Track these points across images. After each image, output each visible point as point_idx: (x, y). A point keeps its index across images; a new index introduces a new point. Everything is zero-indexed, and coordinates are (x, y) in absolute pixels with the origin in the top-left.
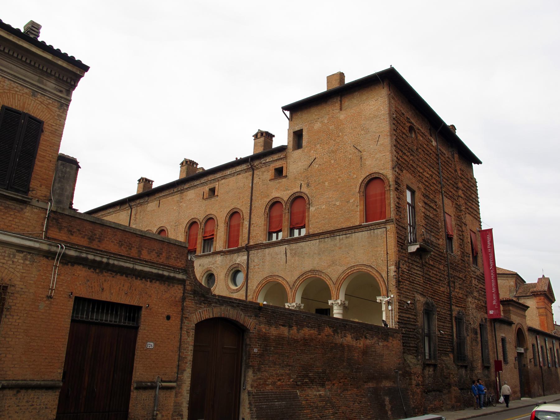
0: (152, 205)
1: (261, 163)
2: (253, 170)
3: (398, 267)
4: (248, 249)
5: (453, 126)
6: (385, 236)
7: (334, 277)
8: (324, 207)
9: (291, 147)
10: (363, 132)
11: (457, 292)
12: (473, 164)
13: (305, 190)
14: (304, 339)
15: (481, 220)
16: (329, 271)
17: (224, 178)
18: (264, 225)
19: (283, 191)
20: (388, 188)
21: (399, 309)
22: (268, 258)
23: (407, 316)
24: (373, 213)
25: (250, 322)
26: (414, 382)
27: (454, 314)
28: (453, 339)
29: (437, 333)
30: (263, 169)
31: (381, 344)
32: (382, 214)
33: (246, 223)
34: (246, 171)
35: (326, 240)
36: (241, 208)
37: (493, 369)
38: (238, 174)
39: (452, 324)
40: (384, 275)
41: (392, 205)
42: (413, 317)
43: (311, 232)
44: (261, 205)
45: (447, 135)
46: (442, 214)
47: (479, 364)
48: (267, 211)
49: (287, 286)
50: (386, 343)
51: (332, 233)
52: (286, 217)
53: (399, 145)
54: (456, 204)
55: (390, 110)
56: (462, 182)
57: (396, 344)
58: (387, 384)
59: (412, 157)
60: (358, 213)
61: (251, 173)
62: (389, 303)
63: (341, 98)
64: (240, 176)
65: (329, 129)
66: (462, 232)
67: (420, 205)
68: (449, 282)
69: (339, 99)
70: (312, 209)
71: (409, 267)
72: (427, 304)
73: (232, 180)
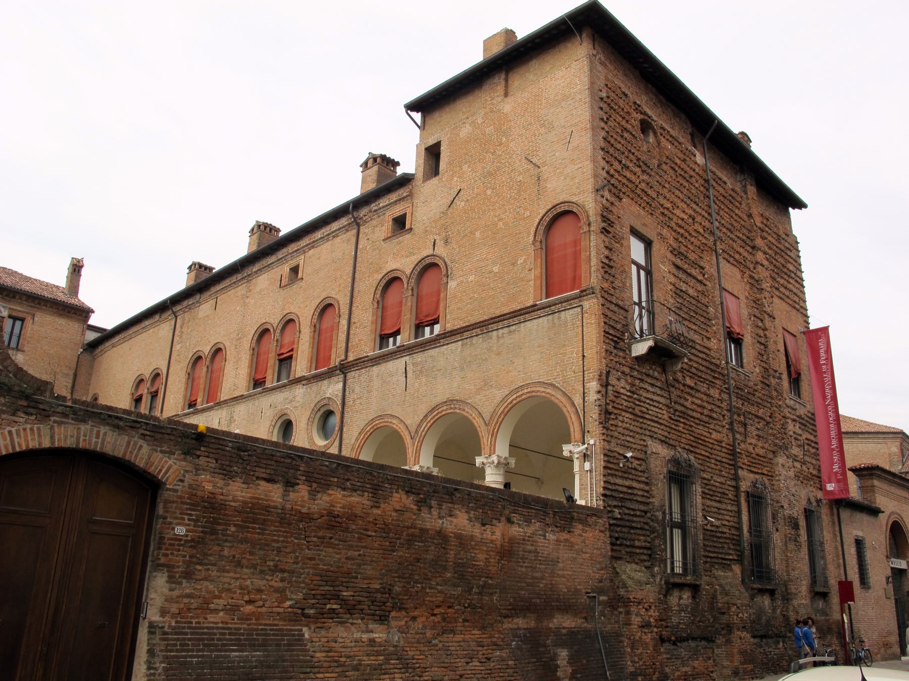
0: (205, 308)
1: (370, 211)
2: (358, 225)
3: (605, 385)
4: (344, 368)
5: (743, 133)
6: (579, 323)
7: (487, 412)
8: (472, 278)
9: (420, 176)
10: (542, 130)
11: (752, 444)
12: (790, 209)
13: (441, 250)
14: (330, 514)
15: (809, 313)
16: (477, 400)
17: (312, 246)
18: (372, 323)
19: (403, 259)
20: (586, 229)
21: (605, 468)
22: (376, 383)
23: (627, 483)
24: (558, 283)
25: (168, 467)
26: (636, 620)
27: (744, 486)
28: (740, 535)
29: (700, 520)
30: (374, 222)
31: (551, 537)
32: (575, 281)
33: (344, 322)
34: (346, 228)
35: (475, 340)
36: (338, 297)
37: (835, 599)
38: (334, 237)
39: (739, 505)
40: (578, 400)
41: (594, 261)
42: (642, 486)
43: (449, 327)
44: (368, 285)
45: (732, 150)
46: (717, 293)
47: (803, 588)
48: (378, 296)
49: (407, 433)
50: (564, 536)
51: (483, 326)
52: (409, 303)
53: (612, 149)
54: (751, 277)
55: (592, 83)
56: (763, 238)
57: (593, 540)
58: (566, 622)
59: (645, 177)
60: (532, 283)
61: (354, 231)
62: (585, 457)
63: (507, 75)
64: (338, 240)
65: (484, 135)
66: (765, 329)
67: (663, 269)
68: (731, 424)
69: (503, 76)
70: (452, 284)
71: (633, 385)
72: (675, 461)
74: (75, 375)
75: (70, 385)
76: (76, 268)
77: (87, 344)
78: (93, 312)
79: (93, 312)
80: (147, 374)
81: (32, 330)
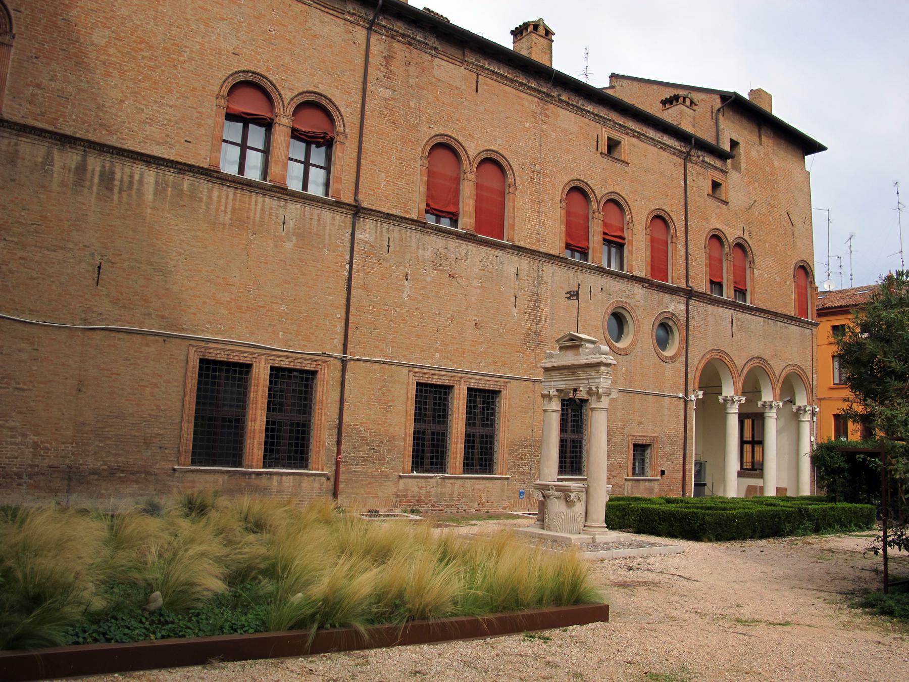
13: (746, 237)
38: (661, 148)
73: (652, 150)
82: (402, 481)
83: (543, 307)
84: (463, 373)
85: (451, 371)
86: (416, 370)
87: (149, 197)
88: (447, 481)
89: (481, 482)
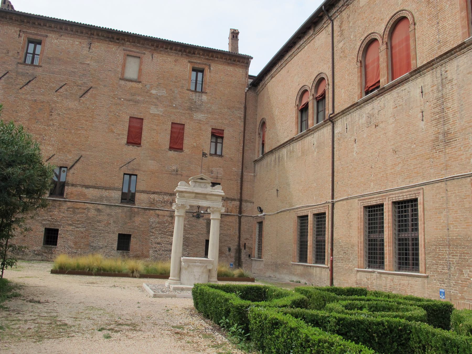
74: (245, 108)
75: (242, 116)
76: (234, 35)
77: (250, 84)
78: (252, 58)
79: (252, 58)
80: (309, 83)
81: (210, 76)
82: (359, 274)
83: (449, 105)
84: (387, 191)
85: (380, 193)
86: (362, 198)
87: (285, 158)
88: (383, 275)
89: (405, 278)
